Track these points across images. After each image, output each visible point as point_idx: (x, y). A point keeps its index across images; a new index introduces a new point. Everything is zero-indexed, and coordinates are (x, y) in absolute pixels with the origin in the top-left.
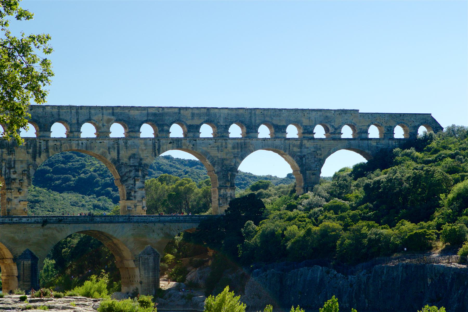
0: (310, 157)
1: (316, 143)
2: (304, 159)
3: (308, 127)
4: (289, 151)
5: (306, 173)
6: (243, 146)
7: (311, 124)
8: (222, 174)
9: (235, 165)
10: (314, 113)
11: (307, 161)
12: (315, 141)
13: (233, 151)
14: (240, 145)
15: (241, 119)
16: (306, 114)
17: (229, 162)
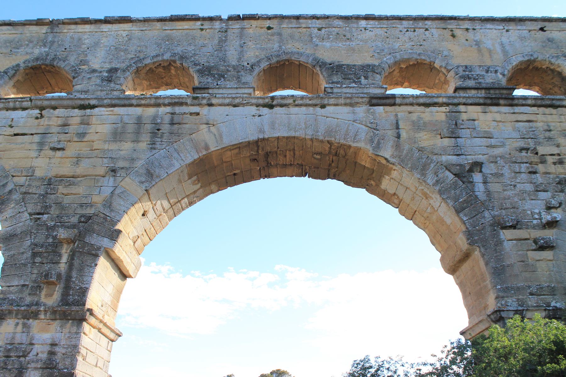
0: (506, 171)
1: (525, 117)
2: (477, 177)
3: (478, 71)
4: (398, 146)
5: (499, 243)
6: (166, 128)
7: (488, 63)
8: (28, 243)
9: (108, 204)
10: (493, 31)
11: (495, 187)
12: (517, 109)
13: (114, 146)
14: (149, 127)
15: (179, 50)
16: (458, 32)
17: (80, 190)
